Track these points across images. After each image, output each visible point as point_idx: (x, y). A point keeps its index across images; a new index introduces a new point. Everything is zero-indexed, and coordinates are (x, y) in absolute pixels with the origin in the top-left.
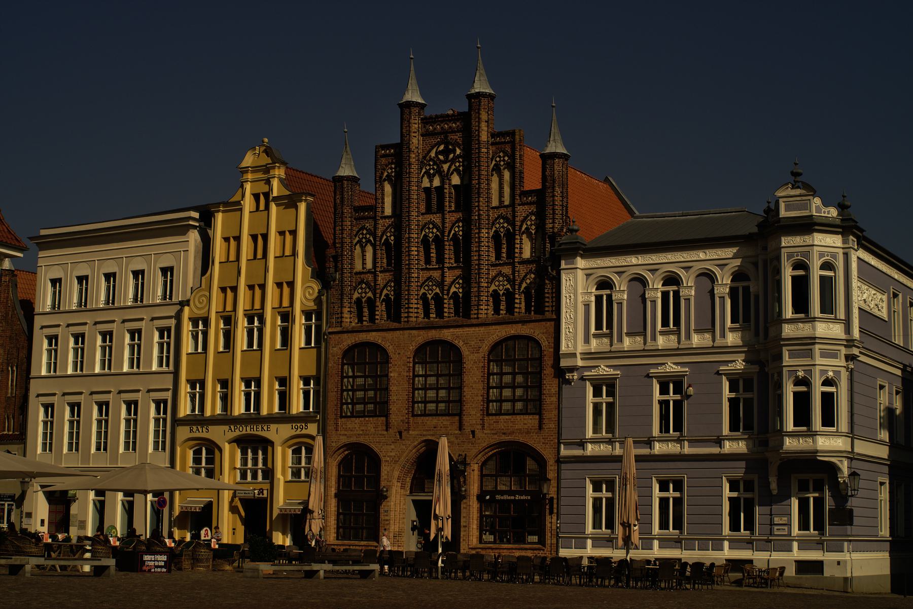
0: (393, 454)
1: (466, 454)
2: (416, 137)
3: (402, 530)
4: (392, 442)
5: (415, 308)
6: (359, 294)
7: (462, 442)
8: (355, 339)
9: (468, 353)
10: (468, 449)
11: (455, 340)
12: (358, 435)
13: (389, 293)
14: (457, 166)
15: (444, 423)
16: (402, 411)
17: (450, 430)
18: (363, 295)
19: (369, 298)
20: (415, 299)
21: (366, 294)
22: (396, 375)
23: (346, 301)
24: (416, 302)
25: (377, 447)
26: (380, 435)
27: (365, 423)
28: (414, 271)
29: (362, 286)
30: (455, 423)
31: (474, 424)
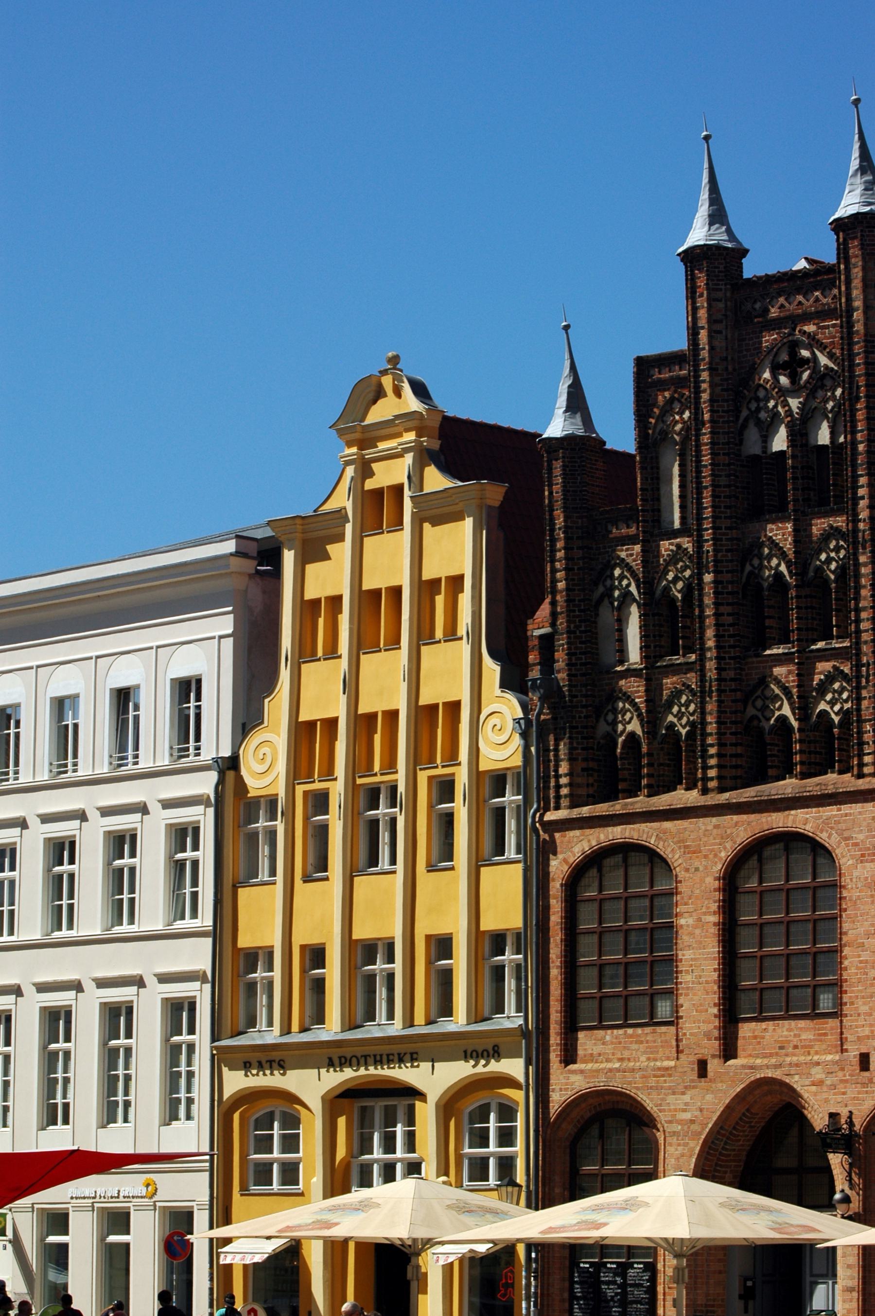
0: (687, 1116)
1: (850, 1112)
2: (720, 332)
3: (714, 1300)
4: (686, 1087)
5: (732, 756)
6: (608, 724)
7: (842, 1081)
9: (850, 862)
10: (858, 1099)
11: (822, 831)
12: (611, 1070)
13: (675, 720)
14: (753, 409)
15: (803, 1037)
16: (707, 1011)
17: (817, 1053)
19: (632, 735)
20: (731, 734)
21: (624, 725)
22: (691, 921)
23: (578, 743)
24: (733, 740)
26: (659, 1069)
28: (725, 664)
30: (825, 1034)
31: (868, 1037)
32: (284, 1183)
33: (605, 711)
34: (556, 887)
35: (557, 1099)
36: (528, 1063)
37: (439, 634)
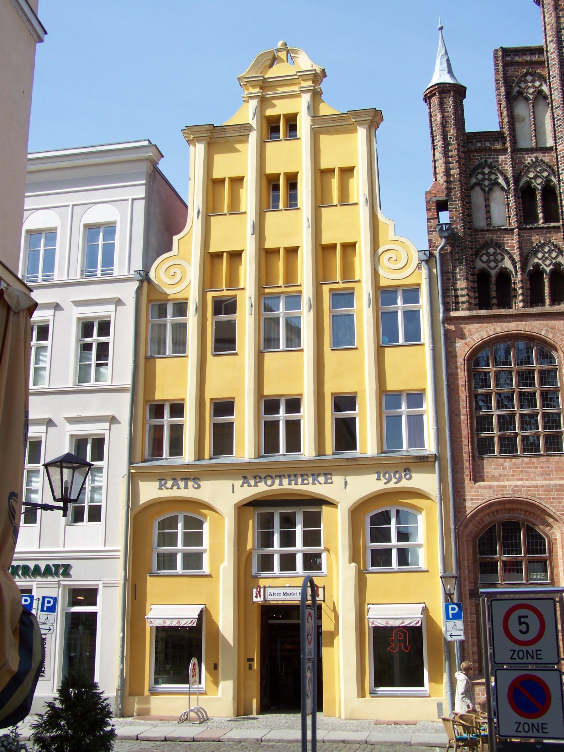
8: (495, 329)
12: (516, 486)
13: (540, 262)
18: (492, 264)
25: (554, 507)
26: (560, 485)
27: (523, 468)
29: (489, 251)
32: (185, 567)
33: (481, 254)
34: (460, 360)
35: (471, 506)
36: (442, 480)
37: (335, 200)
